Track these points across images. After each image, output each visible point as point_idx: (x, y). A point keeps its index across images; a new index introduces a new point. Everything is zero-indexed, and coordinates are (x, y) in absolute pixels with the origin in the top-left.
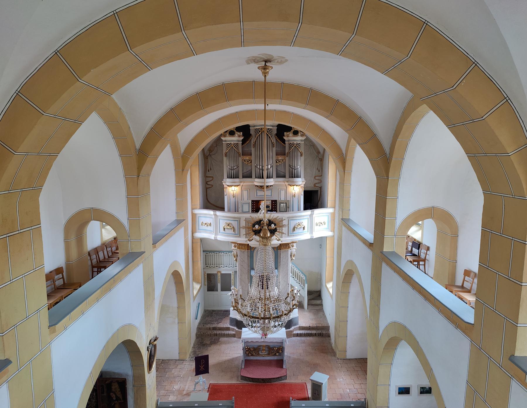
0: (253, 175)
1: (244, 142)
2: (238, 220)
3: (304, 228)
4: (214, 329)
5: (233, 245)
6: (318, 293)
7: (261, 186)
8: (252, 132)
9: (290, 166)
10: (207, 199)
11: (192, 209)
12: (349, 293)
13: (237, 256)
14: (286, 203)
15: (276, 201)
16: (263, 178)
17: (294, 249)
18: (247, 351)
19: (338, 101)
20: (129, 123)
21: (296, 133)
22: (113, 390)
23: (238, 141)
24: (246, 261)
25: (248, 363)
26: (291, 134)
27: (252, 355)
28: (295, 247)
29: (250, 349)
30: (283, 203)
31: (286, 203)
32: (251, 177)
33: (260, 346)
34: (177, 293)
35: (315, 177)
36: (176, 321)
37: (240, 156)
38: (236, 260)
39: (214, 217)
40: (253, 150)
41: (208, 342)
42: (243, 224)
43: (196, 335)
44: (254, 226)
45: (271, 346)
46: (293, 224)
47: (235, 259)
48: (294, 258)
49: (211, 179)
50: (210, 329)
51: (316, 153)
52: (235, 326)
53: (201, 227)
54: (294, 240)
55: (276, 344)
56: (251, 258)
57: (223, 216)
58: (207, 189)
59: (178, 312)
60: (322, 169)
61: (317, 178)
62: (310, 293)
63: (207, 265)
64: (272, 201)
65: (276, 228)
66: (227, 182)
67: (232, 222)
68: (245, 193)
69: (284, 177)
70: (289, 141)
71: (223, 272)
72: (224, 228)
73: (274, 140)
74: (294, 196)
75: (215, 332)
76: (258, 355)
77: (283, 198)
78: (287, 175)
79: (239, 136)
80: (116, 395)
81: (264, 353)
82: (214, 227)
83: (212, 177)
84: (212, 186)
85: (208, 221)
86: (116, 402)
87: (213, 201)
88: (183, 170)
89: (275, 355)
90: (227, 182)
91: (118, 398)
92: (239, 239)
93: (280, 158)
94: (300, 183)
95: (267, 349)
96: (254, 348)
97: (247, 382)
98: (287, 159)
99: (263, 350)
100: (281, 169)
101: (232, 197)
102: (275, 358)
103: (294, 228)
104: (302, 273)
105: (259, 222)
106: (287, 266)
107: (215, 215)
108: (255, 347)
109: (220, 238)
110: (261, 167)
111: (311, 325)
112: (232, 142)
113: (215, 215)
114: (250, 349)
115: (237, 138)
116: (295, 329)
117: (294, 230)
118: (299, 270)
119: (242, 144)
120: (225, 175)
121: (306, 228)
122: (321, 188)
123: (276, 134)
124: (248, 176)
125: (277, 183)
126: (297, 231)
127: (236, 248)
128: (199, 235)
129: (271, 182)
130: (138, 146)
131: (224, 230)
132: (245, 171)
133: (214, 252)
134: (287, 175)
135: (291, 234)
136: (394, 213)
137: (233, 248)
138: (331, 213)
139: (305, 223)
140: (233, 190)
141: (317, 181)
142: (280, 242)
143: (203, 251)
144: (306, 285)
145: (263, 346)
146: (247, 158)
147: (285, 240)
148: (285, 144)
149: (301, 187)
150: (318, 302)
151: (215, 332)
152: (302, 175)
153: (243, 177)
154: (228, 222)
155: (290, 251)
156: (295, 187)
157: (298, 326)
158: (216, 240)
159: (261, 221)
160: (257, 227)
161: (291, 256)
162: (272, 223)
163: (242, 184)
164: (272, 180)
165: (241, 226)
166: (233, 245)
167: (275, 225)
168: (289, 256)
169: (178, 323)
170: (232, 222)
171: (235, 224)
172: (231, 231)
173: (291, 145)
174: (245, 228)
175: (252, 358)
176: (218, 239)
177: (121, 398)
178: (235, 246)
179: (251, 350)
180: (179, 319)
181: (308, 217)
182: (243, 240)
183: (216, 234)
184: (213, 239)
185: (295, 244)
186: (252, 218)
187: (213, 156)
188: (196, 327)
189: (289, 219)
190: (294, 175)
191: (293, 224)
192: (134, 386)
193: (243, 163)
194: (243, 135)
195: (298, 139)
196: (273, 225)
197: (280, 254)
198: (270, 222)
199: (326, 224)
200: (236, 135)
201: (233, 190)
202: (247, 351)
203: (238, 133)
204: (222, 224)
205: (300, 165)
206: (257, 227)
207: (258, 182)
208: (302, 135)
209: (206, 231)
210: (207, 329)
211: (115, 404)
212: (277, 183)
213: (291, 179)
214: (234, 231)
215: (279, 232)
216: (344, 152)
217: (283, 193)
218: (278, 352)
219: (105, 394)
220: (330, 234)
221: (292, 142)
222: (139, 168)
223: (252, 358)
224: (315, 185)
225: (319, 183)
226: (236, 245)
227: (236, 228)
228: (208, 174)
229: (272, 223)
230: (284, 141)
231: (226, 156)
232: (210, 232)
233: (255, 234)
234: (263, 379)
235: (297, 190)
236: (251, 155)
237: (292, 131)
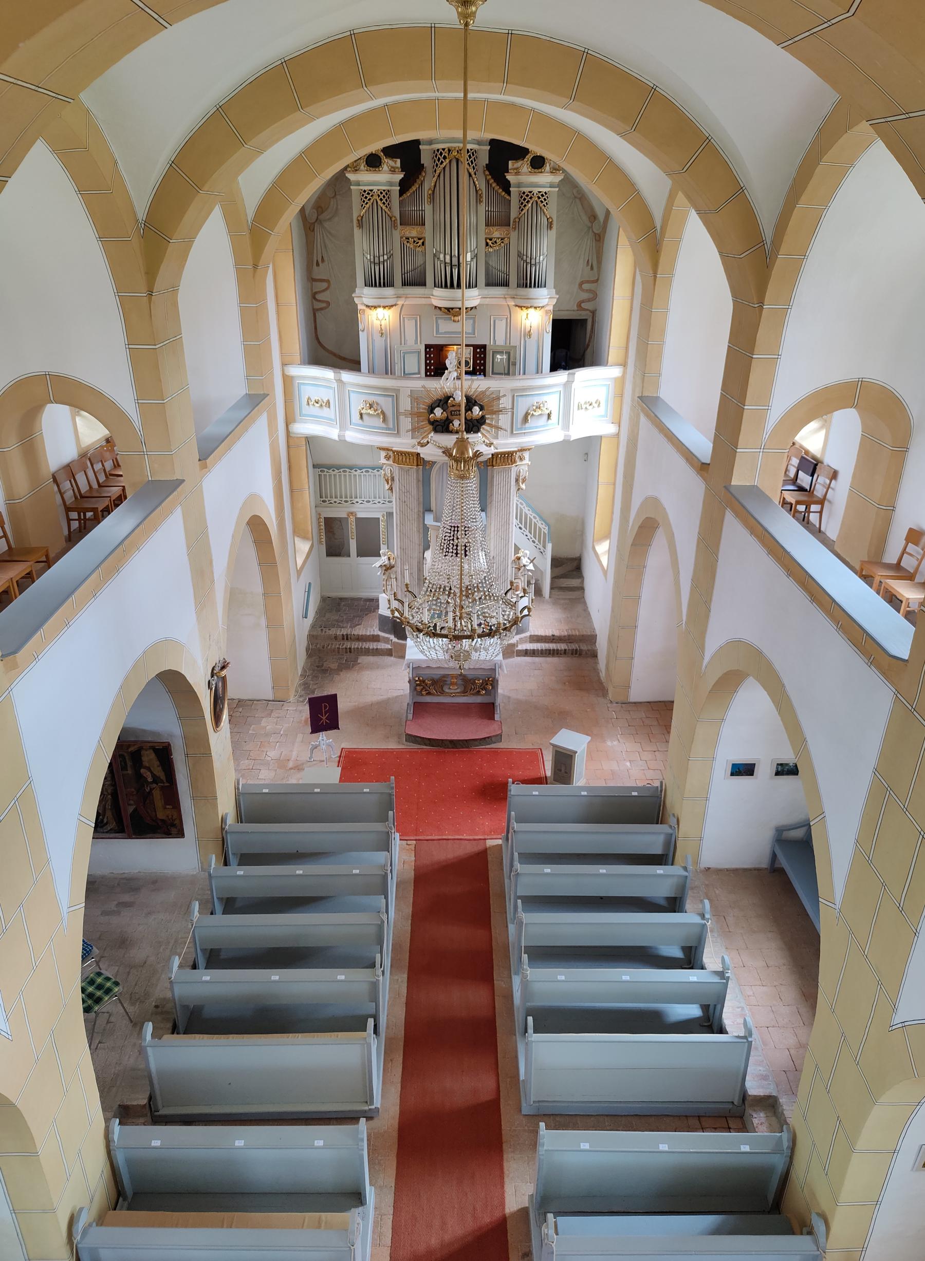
0: (430, 280)
1: (404, 186)
2: (394, 394)
3: (549, 416)
4: (346, 638)
5: (383, 454)
6: (575, 564)
7: (449, 309)
8: (426, 159)
9: (520, 255)
10: (317, 339)
11: (284, 365)
12: (644, 567)
13: (393, 479)
14: (508, 354)
15: (484, 347)
16: (452, 286)
17: (523, 466)
19: (654, 89)
20: (113, 148)
21: (538, 163)
22: (146, 764)
23: (391, 184)
24: (414, 492)
25: (419, 709)
26: (524, 165)
27: (429, 694)
29: (424, 681)
30: (501, 353)
31: (508, 354)
32: (423, 284)
33: (445, 676)
34: (260, 564)
35: (581, 284)
36: (263, 622)
37: (395, 227)
38: (391, 489)
39: (335, 385)
40: (428, 208)
41: (334, 666)
42: (406, 404)
43: (307, 650)
44: (431, 410)
45: (470, 677)
46: (522, 406)
47: (387, 487)
48: (523, 486)
49: (325, 285)
50: (336, 638)
51: (585, 218)
52: (390, 633)
53: (306, 410)
54: (525, 446)
55: (480, 672)
56: (425, 483)
57: (358, 385)
58: (315, 312)
59: (266, 606)
60: (599, 262)
61: (585, 286)
62: (556, 562)
63: (323, 498)
64: (475, 347)
65: (483, 417)
66: (365, 295)
67: (380, 400)
68: (410, 326)
69: (506, 284)
70: (519, 185)
71: (360, 515)
72: (361, 415)
73: (481, 184)
74: (529, 334)
75: (348, 644)
76: (442, 693)
77: (500, 341)
78: (513, 280)
79: (393, 171)
80: (152, 773)
81: (455, 689)
82: (335, 409)
83: (328, 281)
84: (328, 303)
85: (324, 394)
86: (154, 785)
87: (333, 346)
88: (255, 266)
90: (365, 295)
91: (156, 780)
92: (398, 440)
93: (497, 233)
94: (546, 301)
95: (460, 682)
96: (433, 680)
97: (419, 747)
98: (514, 235)
99: (452, 684)
100: (497, 264)
101: (377, 336)
102: (478, 699)
104: (542, 519)
105: (444, 401)
106: (508, 504)
107: (339, 381)
108: (436, 677)
109: (353, 436)
110: (448, 258)
111: (557, 633)
112: (375, 188)
113: (339, 381)
114: (424, 681)
115: (387, 177)
116: (522, 641)
117: (525, 419)
118: (534, 511)
119: (401, 193)
120: (360, 280)
121: (554, 416)
122: (594, 313)
123: (488, 167)
124: (416, 280)
125: (487, 301)
126: (531, 422)
127: (391, 462)
128: (304, 428)
129: (472, 297)
130: (141, 212)
132: (409, 267)
133: (338, 467)
134: (513, 280)
135: (518, 429)
136: (766, 397)
138: (616, 379)
139: (552, 402)
140: (380, 317)
141: (585, 296)
142: (492, 450)
143: (314, 466)
144: (549, 546)
145: (452, 676)
146: (413, 232)
147: (505, 443)
148: (509, 193)
149: (547, 312)
150: (574, 582)
151: (348, 644)
152: (550, 281)
153: (405, 284)
154: (371, 399)
155: (514, 469)
156: (531, 311)
157: (527, 634)
158: (342, 441)
159: (449, 397)
160: (438, 412)
161: (517, 480)
162: (475, 403)
163: (400, 302)
164: (474, 292)
165: (402, 410)
166: (383, 454)
167: (482, 408)
169: (268, 627)
170: (380, 400)
171: (386, 404)
172: (379, 422)
173: (525, 198)
174: (412, 414)
175: (429, 699)
176: (348, 439)
177: (163, 777)
178: (387, 458)
179: (426, 684)
180: (268, 619)
181: (561, 389)
182: (405, 443)
183: (343, 427)
184: (336, 438)
186: (428, 391)
187: (326, 225)
188: (307, 633)
189: (516, 394)
190: (528, 281)
191: (522, 406)
192: (187, 755)
193: (402, 246)
194: (403, 168)
195: (544, 180)
196: (476, 410)
197: (493, 477)
198: (471, 402)
199: (603, 404)
200: (385, 167)
201: (380, 317)
202: (417, 685)
203: (391, 162)
204: (357, 403)
205: (545, 251)
206: (438, 412)
207: (440, 297)
208: (555, 170)
209: (317, 419)
210: (329, 637)
211: (151, 790)
212: (487, 301)
213: (523, 291)
214: (385, 420)
215: (490, 425)
216: (658, 224)
217: (501, 326)
218: (484, 689)
219: (130, 772)
220: (611, 429)
221: (526, 190)
222: (151, 274)
223: (429, 699)
224: (579, 305)
225: (589, 300)
226: (391, 453)
227: (389, 414)
228: (319, 273)
229: (475, 403)
230: (506, 186)
231: (360, 224)
232: (329, 422)
233: (436, 430)
234: (451, 741)
235: (535, 319)
236: (423, 224)
237: (529, 157)
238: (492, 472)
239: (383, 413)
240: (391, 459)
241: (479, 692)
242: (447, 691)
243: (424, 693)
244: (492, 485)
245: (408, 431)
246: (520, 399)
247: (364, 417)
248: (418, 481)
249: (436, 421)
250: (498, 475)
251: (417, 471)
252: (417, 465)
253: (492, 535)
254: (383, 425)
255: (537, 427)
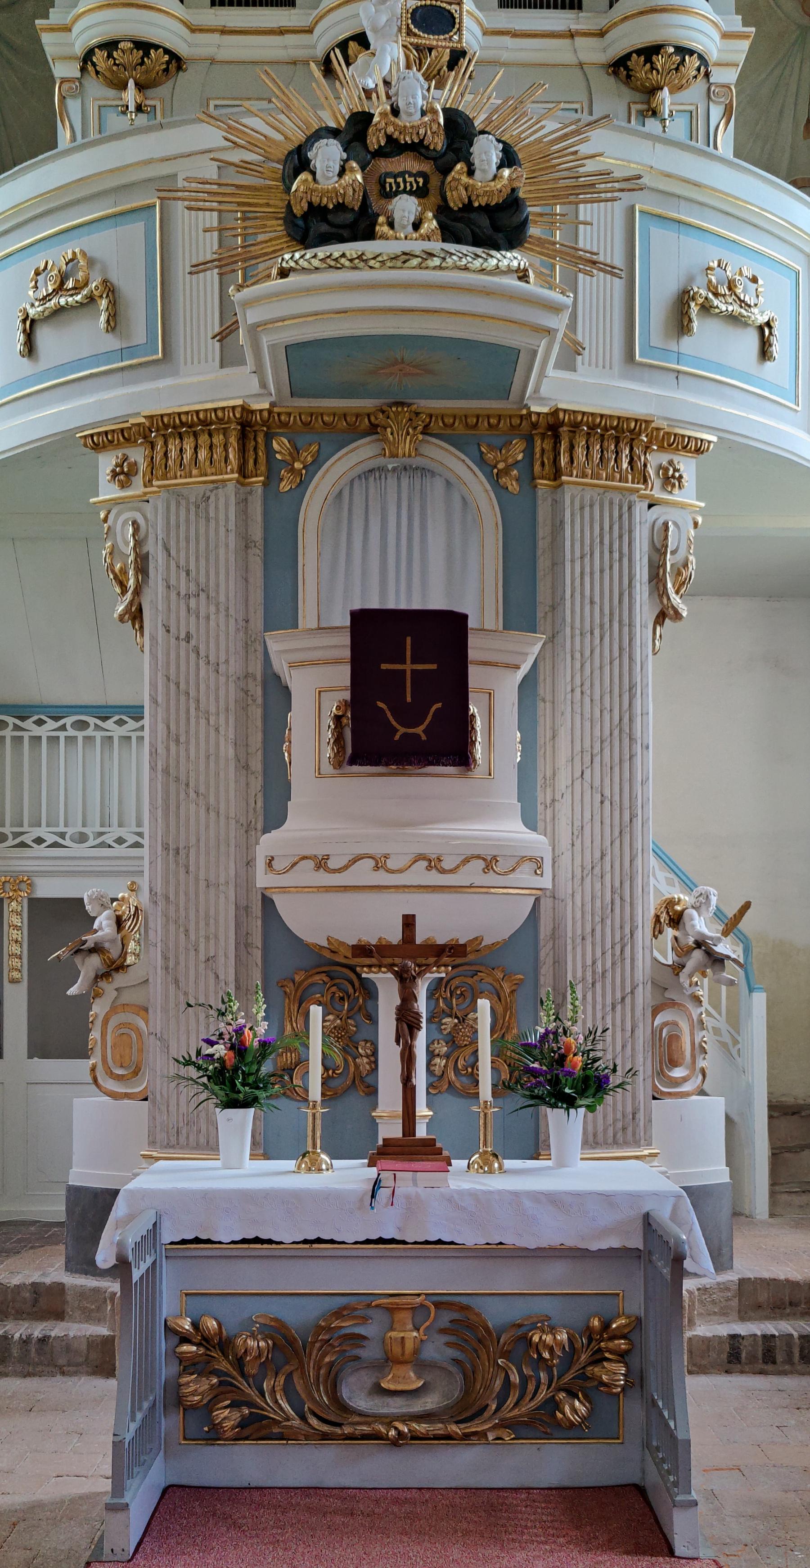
5: (107, 462)
17: (687, 507)
18: (188, 1365)
24: (227, 586)
27: (257, 1428)
28: (687, 495)
45: (495, 1315)
55: (554, 1277)
56: (277, 553)
65: (513, 202)
67: (101, 244)
76: (337, 1424)
89: (544, 1424)
95: (437, 1350)
102: (550, 1463)
103: (684, 299)
108: (298, 1316)
114: (222, 1344)
131: (30, 347)
137: (109, 491)
145: (392, 1307)
166: (107, 462)
168: (642, 572)
170: (101, 244)
178: (123, 474)
185: (687, 466)
197: (557, 528)
202: (188, 1365)
206: (328, 155)
214: (114, 323)
218: (581, 1386)
226: (138, 455)
238: (557, 505)
239: (110, 289)
240: (138, 480)
241: (553, 1405)
242: (361, 1402)
243: (227, 1417)
244: (557, 564)
245: (198, 268)
246: (657, 232)
247: (44, 336)
248: (246, 544)
249: (316, 211)
250: (579, 500)
251: (243, 503)
252: (243, 471)
253: (563, 780)
254: (112, 343)
255: (721, 368)
